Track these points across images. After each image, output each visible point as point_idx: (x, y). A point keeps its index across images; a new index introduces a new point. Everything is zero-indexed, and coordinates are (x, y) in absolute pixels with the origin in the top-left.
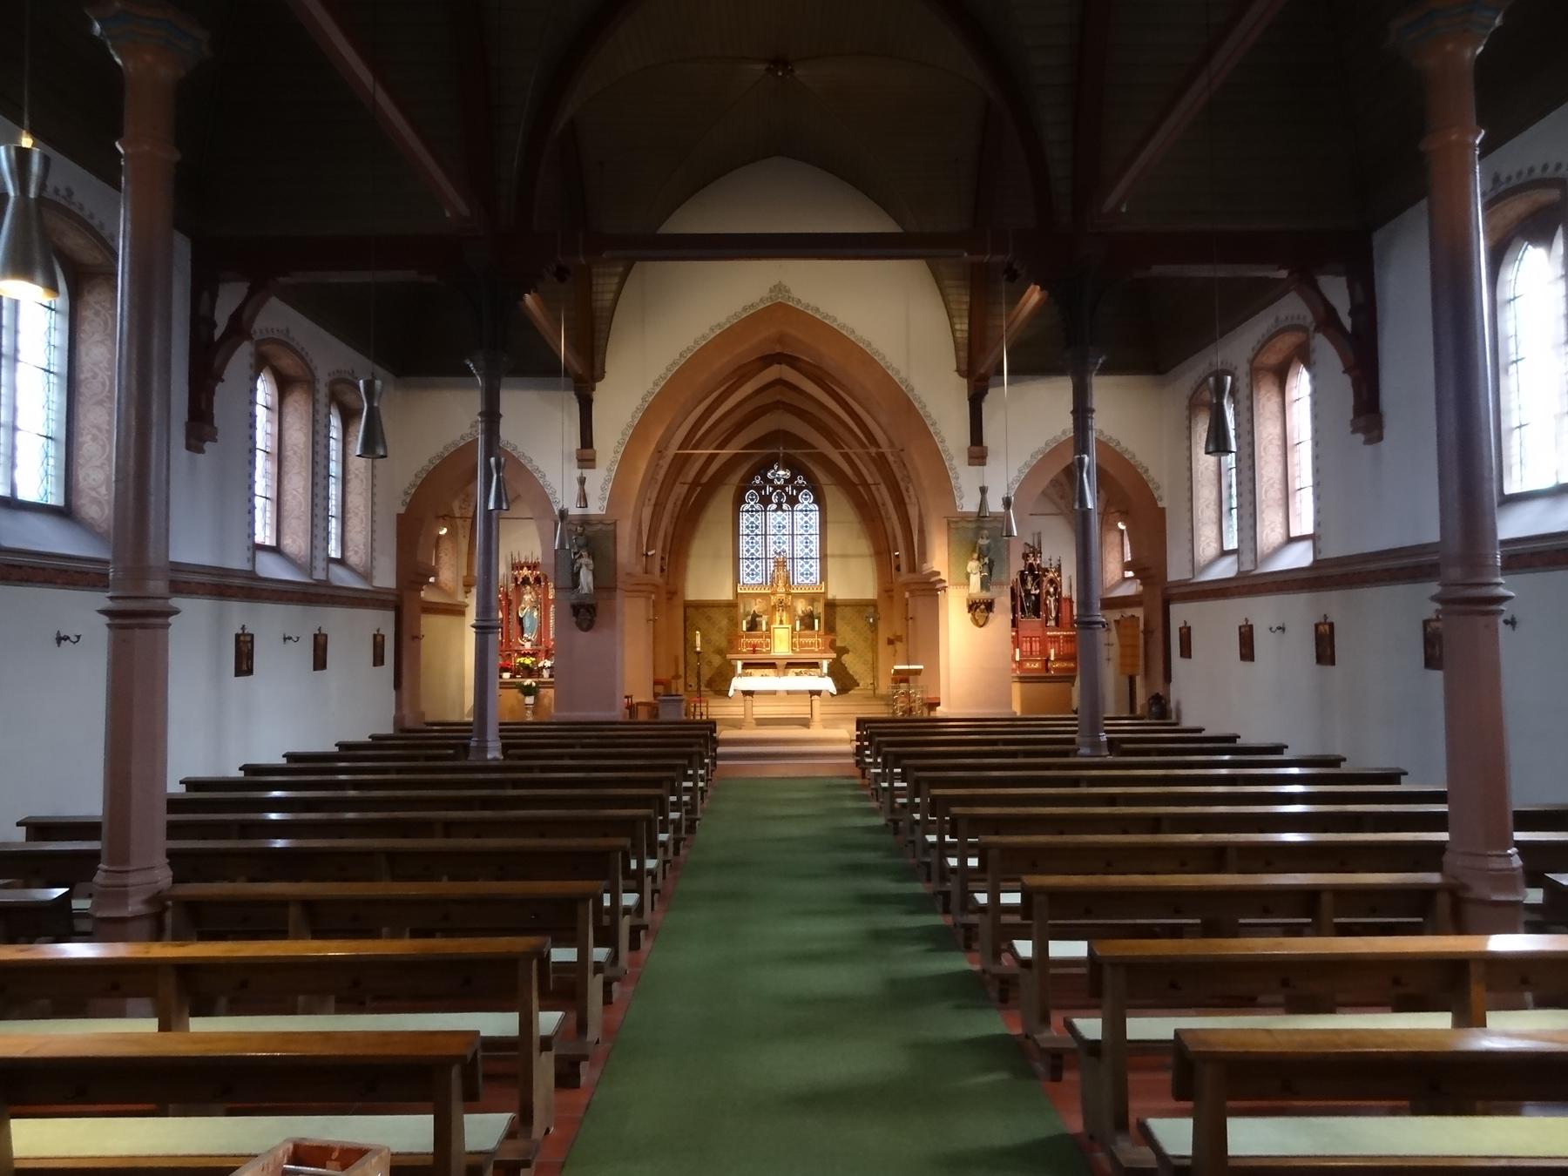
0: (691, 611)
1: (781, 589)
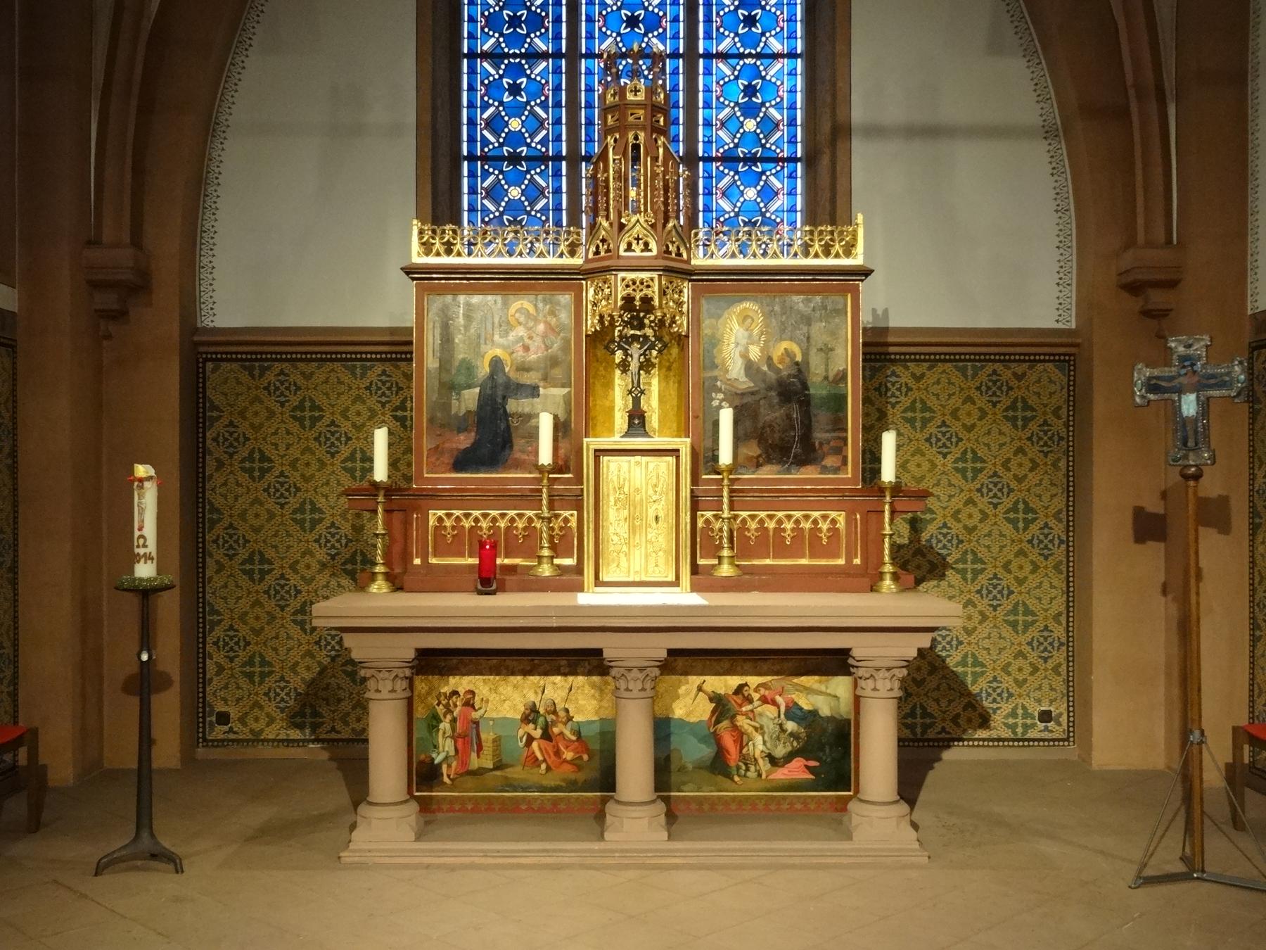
0: (224, 382)
1: (639, 240)
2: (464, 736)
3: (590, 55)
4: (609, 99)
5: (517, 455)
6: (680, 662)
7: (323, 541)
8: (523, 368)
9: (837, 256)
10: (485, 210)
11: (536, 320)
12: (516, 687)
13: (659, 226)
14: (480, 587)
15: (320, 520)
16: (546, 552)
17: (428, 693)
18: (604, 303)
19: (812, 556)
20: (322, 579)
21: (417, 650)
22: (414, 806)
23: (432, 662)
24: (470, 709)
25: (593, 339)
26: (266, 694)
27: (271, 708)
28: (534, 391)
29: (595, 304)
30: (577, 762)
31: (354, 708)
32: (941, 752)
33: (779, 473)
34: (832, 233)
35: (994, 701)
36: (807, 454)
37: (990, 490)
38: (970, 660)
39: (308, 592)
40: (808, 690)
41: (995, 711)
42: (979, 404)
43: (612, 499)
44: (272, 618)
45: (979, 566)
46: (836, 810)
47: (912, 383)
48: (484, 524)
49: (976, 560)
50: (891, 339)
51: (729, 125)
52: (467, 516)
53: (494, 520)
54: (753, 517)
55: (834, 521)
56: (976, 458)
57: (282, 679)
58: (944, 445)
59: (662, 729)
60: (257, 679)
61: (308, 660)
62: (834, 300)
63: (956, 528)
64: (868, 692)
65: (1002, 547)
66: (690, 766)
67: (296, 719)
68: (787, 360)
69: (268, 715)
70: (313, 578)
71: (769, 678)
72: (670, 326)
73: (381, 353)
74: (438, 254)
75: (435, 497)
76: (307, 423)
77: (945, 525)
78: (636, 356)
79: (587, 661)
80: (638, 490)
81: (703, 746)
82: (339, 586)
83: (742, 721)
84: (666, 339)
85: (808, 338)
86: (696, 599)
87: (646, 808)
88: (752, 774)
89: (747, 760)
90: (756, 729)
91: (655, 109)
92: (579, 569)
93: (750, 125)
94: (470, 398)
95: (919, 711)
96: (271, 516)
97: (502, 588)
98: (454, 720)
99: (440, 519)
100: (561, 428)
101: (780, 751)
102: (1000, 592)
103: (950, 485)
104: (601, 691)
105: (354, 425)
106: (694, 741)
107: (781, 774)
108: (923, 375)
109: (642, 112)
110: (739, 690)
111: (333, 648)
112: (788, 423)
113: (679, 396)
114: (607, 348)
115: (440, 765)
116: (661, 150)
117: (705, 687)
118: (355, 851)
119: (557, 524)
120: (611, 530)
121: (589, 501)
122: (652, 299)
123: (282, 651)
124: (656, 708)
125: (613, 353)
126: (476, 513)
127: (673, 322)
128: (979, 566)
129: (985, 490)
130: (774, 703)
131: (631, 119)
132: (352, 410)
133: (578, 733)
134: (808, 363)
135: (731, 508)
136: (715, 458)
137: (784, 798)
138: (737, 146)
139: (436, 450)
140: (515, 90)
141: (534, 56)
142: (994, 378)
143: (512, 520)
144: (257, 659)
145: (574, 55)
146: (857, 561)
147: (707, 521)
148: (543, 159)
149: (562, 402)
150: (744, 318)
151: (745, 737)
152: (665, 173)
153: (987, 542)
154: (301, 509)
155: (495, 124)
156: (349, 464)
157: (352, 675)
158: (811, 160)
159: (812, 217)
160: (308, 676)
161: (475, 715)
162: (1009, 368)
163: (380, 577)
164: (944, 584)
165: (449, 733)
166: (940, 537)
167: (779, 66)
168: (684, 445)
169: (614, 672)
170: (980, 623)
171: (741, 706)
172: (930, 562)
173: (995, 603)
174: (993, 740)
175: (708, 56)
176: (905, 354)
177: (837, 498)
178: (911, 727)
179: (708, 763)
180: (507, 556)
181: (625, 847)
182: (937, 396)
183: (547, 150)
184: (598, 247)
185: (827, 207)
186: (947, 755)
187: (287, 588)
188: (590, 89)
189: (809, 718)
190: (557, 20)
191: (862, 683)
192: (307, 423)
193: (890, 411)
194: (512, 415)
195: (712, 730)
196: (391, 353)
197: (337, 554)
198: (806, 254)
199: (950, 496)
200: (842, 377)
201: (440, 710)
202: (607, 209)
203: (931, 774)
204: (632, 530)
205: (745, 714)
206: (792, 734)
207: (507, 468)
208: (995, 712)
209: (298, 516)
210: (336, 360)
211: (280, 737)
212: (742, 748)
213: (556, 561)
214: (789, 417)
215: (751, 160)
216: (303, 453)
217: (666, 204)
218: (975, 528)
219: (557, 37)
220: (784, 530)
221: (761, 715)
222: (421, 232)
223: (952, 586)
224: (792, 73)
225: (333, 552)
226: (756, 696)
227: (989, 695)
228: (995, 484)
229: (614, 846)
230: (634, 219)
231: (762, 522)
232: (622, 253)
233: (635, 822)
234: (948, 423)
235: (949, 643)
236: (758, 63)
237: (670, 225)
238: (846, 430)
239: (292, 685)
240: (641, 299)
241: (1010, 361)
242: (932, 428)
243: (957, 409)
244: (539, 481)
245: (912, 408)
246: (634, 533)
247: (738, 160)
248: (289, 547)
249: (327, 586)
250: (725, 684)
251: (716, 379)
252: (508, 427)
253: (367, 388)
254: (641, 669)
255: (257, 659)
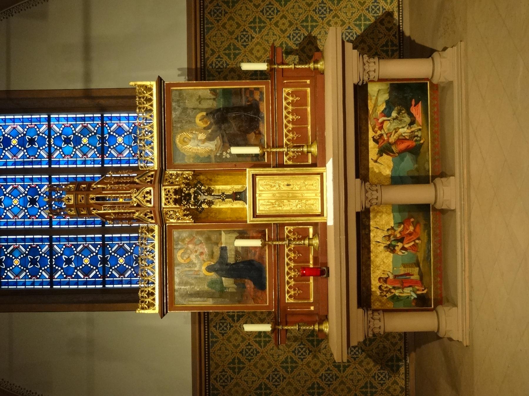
1: (145, 197)
2: (402, 283)
3: (50, 223)
4: (73, 213)
5: (256, 257)
6: (362, 172)
7: (302, 357)
8: (212, 255)
9: (151, 95)
10: (131, 276)
11: (187, 249)
12: (376, 256)
13: (138, 186)
14: (325, 276)
15: (291, 358)
16: (307, 242)
17: (380, 301)
18: (177, 214)
19: (307, 105)
20: (321, 357)
21: (358, 307)
22: (440, 308)
23: (364, 299)
24: (388, 280)
25: (196, 219)
26: (382, 385)
27: (389, 383)
28: (224, 249)
29: (178, 219)
30: (415, 223)
31: (388, 340)
32: (405, 36)
33: (263, 123)
34: (140, 98)
35: (379, 9)
36: (254, 109)
37: (270, 14)
38: (358, 23)
39: (328, 364)
40: (376, 105)
41: (384, 9)
42: (226, 21)
43: (278, 208)
44: (342, 382)
45: (309, 19)
46: (437, 90)
47: (216, 55)
48: (293, 274)
49: (306, 20)
50: (194, 67)
51: (85, 130)
52: (288, 283)
53: (290, 269)
54: (287, 136)
55: (288, 94)
56: (254, 22)
57: (374, 377)
58: (247, 38)
59: (397, 180)
60: (374, 390)
61: (364, 364)
62: (174, 96)
63: (290, 31)
64: (376, 75)
65: (300, 7)
66: (416, 166)
67: (395, 370)
68: (205, 119)
69: (393, 384)
70: (321, 362)
71: (369, 126)
72: (189, 180)
73: (205, 328)
74: (154, 300)
75: (279, 299)
76: (241, 366)
77: (289, 37)
78: (205, 197)
79: (363, 219)
80: (274, 195)
81: (405, 159)
82: (325, 348)
83: (392, 139)
84: (195, 182)
85: (194, 109)
86: (330, 164)
87: (438, 188)
88: (419, 133)
89: (412, 136)
90: (396, 132)
91: (78, 189)
92: (315, 225)
93: (85, 140)
94: (228, 282)
95: (385, 48)
96: (289, 383)
97: (326, 264)
98: (394, 288)
99: (290, 297)
100: (242, 235)
101: (407, 119)
102: (322, 8)
103: (268, 34)
104: (378, 212)
105: (242, 342)
106: (403, 164)
107: (419, 118)
108: (212, 50)
109: (79, 196)
110: (375, 140)
111: (358, 351)
112: (237, 119)
113: (226, 174)
114: (201, 212)
115: (417, 295)
116: (99, 186)
117: (375, 158)
118: (463, 338)
119: (292, 237)
120: (294, 208)
121: (280, 220)
122: (175, 189)
123: (359, 377)
124: (386, 184)
125: (203, 209)
126: (287, 278)
127: (186, 178)
128: (309, 19)
129: (270, 17)
130: (382, 123)
131: (83, 202)
132: (235, 342)
133: (400, 224)
134: (207, 109)
135: (282, 147)
136: (256, 155)
137: (431, 116)
138: (96, 147)
139: (255, 299)
140: (69, 261)
141: (51, 251)
142: (212, 13)
143: (290, 259)
144: (364, 390)
145: (51, 231)
146: (308, 82)
147: (289, 159)
148: (104, 247)
149: (229, 235)
150: (184, 142)
151: (401, 138)
152: (111, 184)
153: (297, 15)
154: (286, 368)
155: (86, 271)
156: (262, 344)
157: (371, 341)
158: (102, 109)
159: (132, 108)
160: (372, 364)
161: (391, 277)
162: (207, 6)
163: (321, 327)
164: (319, 37)
165: (401, 290)
166: (295, 39)
167: (54, 126)
168: (250, 172)
169: (368, 206)
170: (338, 17)
171: (384, 140)
172: (308, 44)
173: (328, 10)
174: (399, 10)
175: (50, 163)
176: (201, 59)
177: (276, 91)
178: (393, 51)
179: (414, 156)
180: (309, 262)
181: (458, 198)
182: (222, 42)
183: (99, 244)
184: (149, 218)
185: (126, 100)
186: (407, 33)
187: (327, 375)
188: (68, 223)
189: (390, 105)
190: (33, 240)
191: (371, 78)
192: (241, 366)
193: (230, 66)
194: (236, 260)
195: (397, 155)
196: (205, 323)
197: (309, 350)
198: (151, 111)
199: (274, 34)
200: (214, 91)
201: (389, 295)
202: (130, 213)
203: (417, 41)
204: (294, 198)
205: (389, 137)
206: (399, 113)
207: (264, 262)
208: (385, 9)
209: (289, 369)
210: (209, 351)
211: (404, 377)
212: (406, 139)
213: (311, 236)
214: (235, 118)
215: (103, 140)
216: (257, 368)
217: (126, 183)
218: (290, 21)
219: (41, 240)
220: (293, 119)
221: (389, 130)
222: (143, 308)
223: (320, 32)
224: (58, 119)
225: (307, 352)
226: (379, 132)
227: (376, 12)
228: (267, 11)
229: (458, 204)
230: (135, 200)
231: (289, 131)
232: (152, 205)
233: (446, 193)
234: (236, 36)
235: (349, 34)
236: (53, 137)
237: (137, 181)
238: (241, 89)
239: (377, 372)
240: (175, 195)
241: (203, 5)
242: (239, 44)
243: (229, 32)
244: (270, 246)
245: (229, 55)
246: (296, 197)
247: (103, 146)
248: (306, 374)
249: (325, 355)
250: (373, 148)
251: (216, 156)
252: (243, 262)
253: (223, 335)
254: (366, 192)
255: (364, 390)
